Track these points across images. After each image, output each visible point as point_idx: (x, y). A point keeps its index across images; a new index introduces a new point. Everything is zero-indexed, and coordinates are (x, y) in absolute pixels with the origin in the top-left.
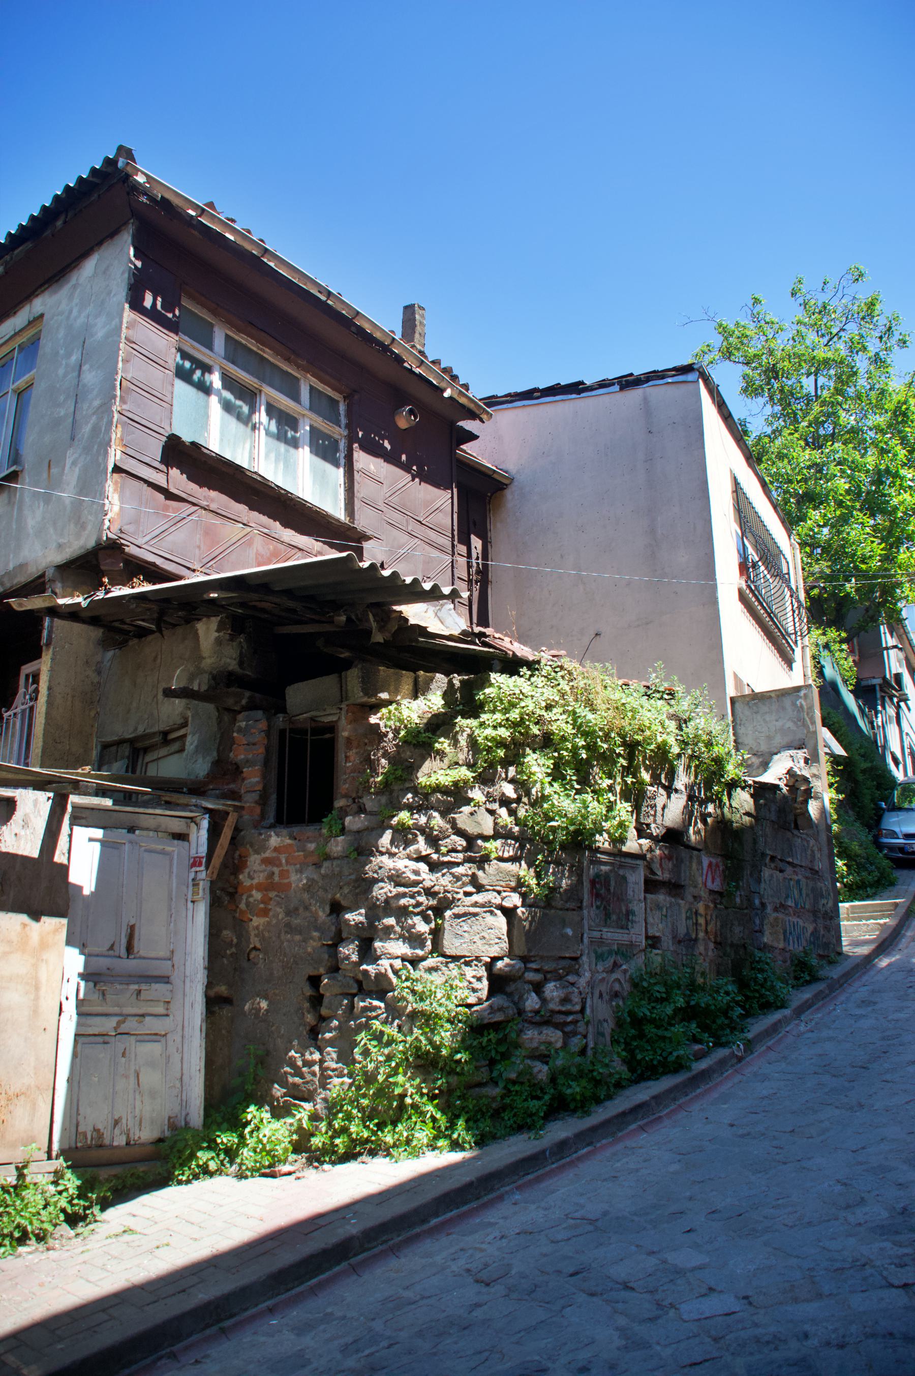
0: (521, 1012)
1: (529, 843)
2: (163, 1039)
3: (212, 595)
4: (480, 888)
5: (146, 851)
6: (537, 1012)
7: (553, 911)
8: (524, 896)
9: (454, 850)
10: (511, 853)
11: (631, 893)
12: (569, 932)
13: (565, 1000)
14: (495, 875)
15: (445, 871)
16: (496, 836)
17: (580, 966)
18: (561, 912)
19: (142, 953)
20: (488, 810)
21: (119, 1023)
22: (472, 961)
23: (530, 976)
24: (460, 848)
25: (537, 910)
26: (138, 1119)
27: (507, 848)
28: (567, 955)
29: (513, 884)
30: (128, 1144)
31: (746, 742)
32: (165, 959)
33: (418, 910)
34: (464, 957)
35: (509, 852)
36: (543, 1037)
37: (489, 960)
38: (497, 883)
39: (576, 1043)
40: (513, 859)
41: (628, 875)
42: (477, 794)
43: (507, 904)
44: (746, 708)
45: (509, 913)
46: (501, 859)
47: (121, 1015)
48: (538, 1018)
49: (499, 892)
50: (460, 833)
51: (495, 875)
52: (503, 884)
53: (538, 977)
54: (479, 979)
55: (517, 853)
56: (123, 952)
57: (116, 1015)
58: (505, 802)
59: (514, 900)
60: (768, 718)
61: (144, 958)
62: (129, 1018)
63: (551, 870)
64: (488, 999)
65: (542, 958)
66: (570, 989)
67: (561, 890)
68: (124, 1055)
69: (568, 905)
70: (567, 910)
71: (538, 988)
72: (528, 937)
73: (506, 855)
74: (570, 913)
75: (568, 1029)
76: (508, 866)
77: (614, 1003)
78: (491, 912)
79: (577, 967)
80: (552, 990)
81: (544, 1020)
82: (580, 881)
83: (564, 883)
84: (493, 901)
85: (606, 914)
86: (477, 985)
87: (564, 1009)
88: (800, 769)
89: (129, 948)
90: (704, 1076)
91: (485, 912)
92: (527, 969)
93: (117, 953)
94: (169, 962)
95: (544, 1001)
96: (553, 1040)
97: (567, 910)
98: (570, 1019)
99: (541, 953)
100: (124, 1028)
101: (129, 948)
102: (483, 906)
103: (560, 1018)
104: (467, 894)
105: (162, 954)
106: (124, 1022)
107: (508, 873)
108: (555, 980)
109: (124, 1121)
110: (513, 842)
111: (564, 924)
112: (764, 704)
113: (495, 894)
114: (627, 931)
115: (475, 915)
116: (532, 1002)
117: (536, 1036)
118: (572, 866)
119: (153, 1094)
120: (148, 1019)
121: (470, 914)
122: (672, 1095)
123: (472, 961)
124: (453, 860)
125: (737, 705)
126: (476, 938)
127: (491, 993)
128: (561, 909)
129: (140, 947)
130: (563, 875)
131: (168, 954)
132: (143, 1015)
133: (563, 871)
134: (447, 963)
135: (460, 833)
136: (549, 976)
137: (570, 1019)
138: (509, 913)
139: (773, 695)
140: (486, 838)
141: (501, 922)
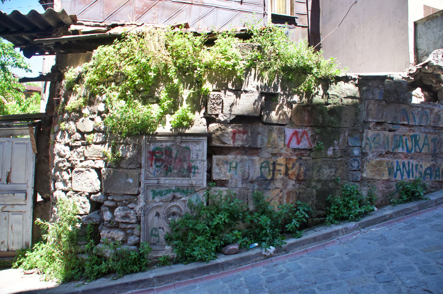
0: (102, 220)
1: (110, 135)
2: (24, 213)
3: (24, 36)
4: (86, 159)
5: (16, 144)
6: (109, 222)
7: (121, 170)
8: (106, 162)
9: (77, 140)
10: (101, 140)
11: (195, 157)
12: (131, 181)
13: (126, 216)
14: (92, 152)
15: (75, 150)
16: (94, 131)
17: (138, 199)
18: (126, 170)
19: (14, 182)
20: (90, 119)
21: (3, 208)
22: (82, 194)
23: (107, 203)
24: (79, 139)
25: (112, 169)
26: (12, 242)
27: (99, 138)
28: (129, 193)
29: (101, 156)
30: (8, 250)
31: (422, 48)
32: (25, 184)
33: (64, 169)
34: (79, 192)
35: (99, 140)
36: (110, 235)
37: (88, 194)
38: (93, 156)
39: (132, 239)
40: (102, 143)
41: (191, 146)
42: (86, 111)
43: (97, 166)
44: (423, 26)
45: (98, 170)
46: (96, 144)
47: (5, 205)
48: (109, 225)
49: (94, 160)
50: (78, 131)
51: (92, 152)
52: (96, 156)
53: (111, 204)
54: (84, 203)
55: (103, 140)
56: (6, 182)
57: (3, 205)
58: (100, 113)
59: (100, 164)
60: (435, 30)
61: (15, 184)
62: (8, 206)
63: (121, 148)
64: (90, 213)
65: (114, 194)
66: (128, 211)
67: (127, 158)
68: (5, 219)
69: (130, 167)
70: (131, 169)
71: (112, 209)
72: (107, 182)
73: (98, 141)
74: (131, 171)
75: (128, 231)
76: (99, 147)
77: (170, 219)
78: (89, 170)
79: (136, 199)
80: (118, 212)
81: (116, 226)
82: (139, 152)
83: (129, 155)
84: (90, 165)
85: (167, 170)
86: (84, 206)
87: (124, 221)
88: (437, 61)
89: (8, 181)
90: (217, 267)
91: (86, 170)
92: (107, 200)
93: (3, 183)
94: (26, 185)
95: (114, 217)
96: (116, 237)
97: (131, 169)
98: (129, 226)
99: (112, 192)
100: (5, 209)
101: (8, 181)
102: (85, 167)
103: (123, 226)
104: (81, 161)
105: (23, 182)
106: (6, 207)
107: (98, 150)
108: (121, 206)
109: (6, 242)
110: (102, 134)
111: (127, 177)
112: (433, 22)
113: (92, 161)
114: (189, 179)
115: (82, 172)
116: (107, 216)
117: (106, 234)
118: (135, 145)
119: (18, 233)
120: (16, 206)
121: (81, 171)
122: (177, 277)
123: (82, 194)
124: (76, 145)
125: (419, 27)
126: (83, 183)
127: (92, 210)
128: (127, 169)
129: (13, 179)
130: (129, 150)
131: (26, 182)
132: (14, 205)
133: (128, 148)
134: (74, 194)
135: (78, 131)
136: (118, 204)
137: (129, 226)
138: (98, 170)
139: (438, 15)
140: (89, 133)
141: (94, 174)
